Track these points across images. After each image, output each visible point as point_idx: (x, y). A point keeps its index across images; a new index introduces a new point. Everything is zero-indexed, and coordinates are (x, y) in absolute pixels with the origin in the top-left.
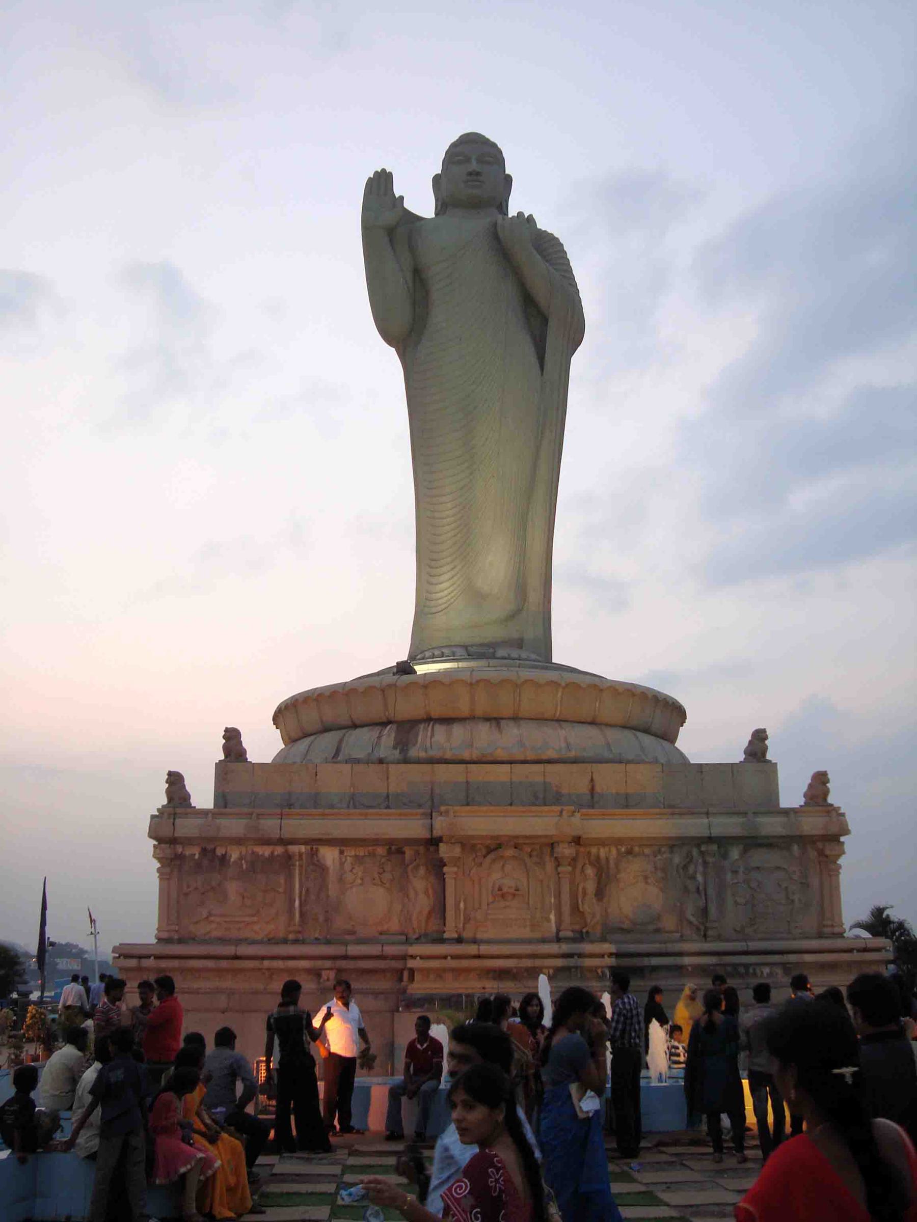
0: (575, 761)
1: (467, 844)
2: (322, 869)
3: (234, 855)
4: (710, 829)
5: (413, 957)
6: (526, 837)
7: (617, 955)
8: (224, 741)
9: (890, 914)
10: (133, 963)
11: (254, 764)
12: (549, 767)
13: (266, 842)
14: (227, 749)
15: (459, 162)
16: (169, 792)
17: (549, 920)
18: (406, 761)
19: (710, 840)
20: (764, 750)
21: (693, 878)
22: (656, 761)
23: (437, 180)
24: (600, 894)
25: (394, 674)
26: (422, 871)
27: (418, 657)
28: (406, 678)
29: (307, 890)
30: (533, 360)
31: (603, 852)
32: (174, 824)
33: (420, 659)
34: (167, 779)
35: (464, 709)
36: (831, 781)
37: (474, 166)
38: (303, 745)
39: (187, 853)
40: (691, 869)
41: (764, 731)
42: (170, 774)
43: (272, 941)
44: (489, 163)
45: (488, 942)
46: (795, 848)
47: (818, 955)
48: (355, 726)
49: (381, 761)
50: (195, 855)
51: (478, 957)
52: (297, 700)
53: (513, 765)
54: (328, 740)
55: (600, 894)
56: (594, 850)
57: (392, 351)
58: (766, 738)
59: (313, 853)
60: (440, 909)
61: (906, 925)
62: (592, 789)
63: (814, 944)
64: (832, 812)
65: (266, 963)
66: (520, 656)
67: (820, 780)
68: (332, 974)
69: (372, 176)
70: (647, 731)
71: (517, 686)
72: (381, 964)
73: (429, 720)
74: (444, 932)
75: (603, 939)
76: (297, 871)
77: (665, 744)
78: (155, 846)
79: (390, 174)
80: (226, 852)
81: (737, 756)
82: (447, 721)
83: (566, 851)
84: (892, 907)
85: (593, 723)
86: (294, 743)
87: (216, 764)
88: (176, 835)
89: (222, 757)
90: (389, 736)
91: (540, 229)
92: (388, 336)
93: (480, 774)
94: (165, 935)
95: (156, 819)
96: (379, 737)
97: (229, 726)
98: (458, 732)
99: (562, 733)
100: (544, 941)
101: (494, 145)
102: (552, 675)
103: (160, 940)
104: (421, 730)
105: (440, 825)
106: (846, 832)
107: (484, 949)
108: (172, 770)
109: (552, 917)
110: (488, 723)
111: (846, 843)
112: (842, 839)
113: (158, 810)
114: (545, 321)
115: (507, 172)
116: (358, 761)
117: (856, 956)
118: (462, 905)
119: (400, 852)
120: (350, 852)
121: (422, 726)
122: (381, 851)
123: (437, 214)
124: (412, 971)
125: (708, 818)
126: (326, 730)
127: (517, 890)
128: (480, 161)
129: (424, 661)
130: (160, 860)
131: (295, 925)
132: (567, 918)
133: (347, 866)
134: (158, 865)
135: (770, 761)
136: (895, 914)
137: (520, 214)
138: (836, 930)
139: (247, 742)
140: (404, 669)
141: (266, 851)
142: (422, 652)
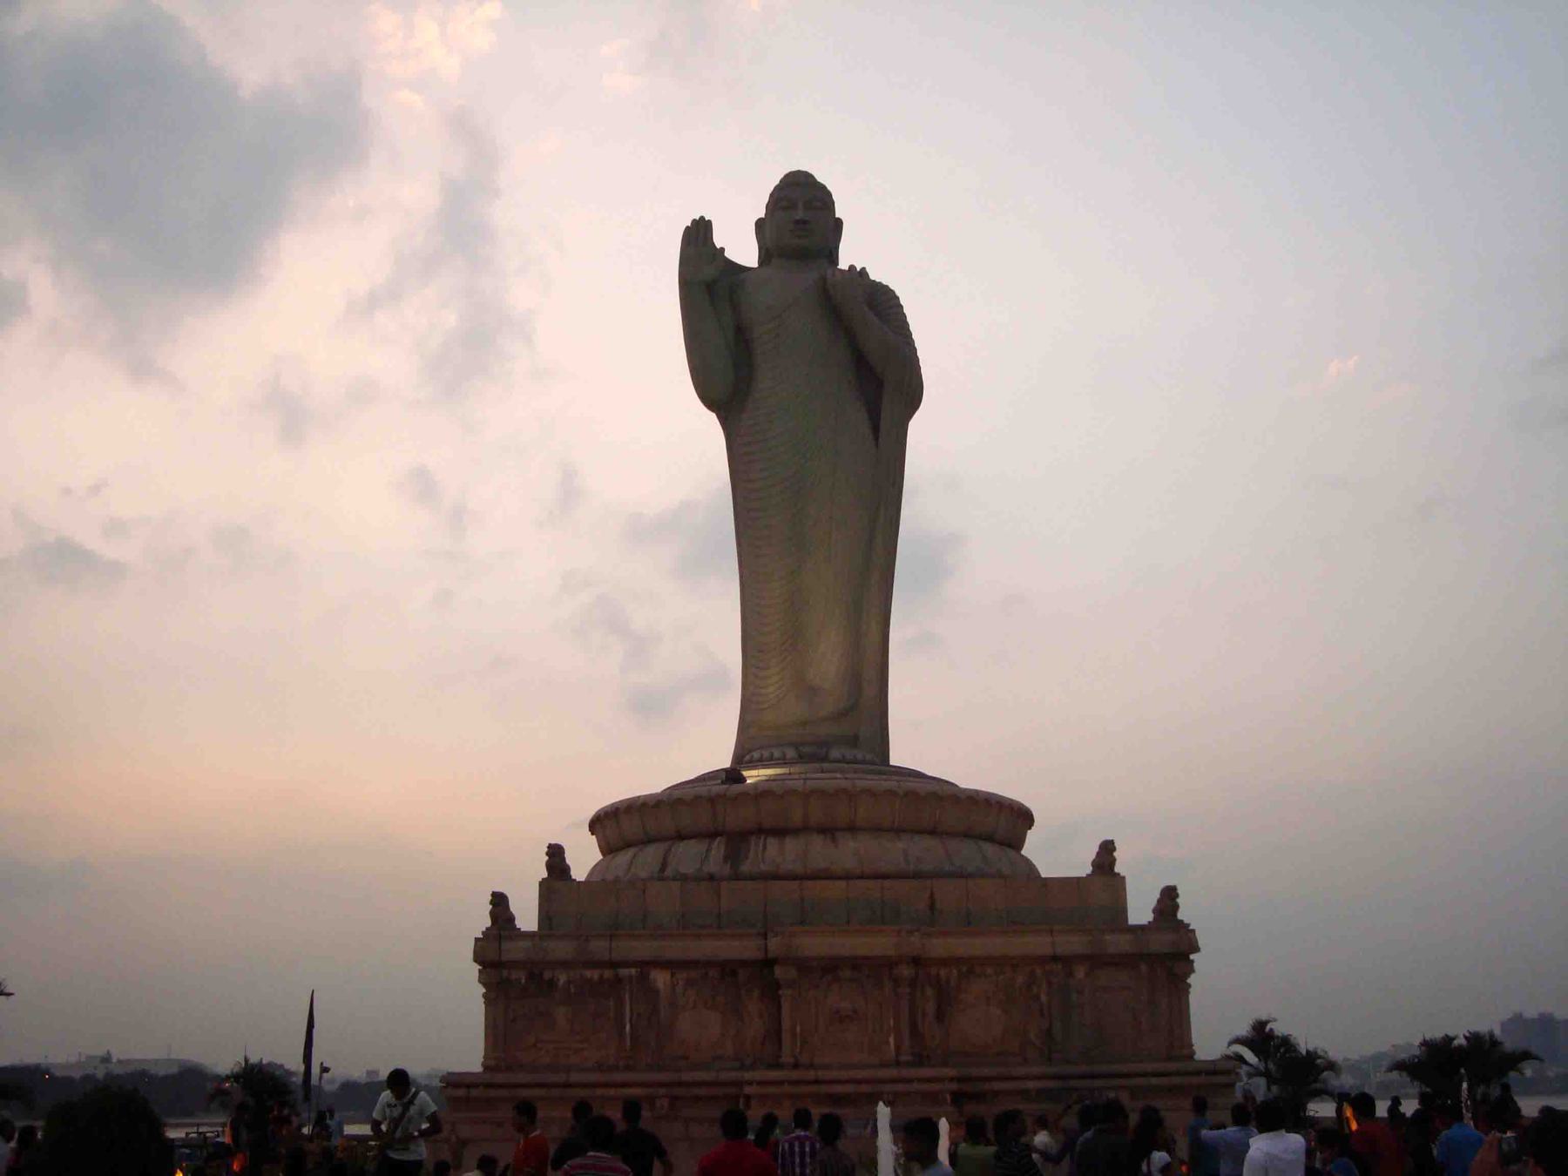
0: (917, 875)
1: (804, 966)
3: (562, 979)
5: (750, 1083)
6: (866, 958)
7: (960, 1080)
9: (1273, 1027)
10: (461, 1092)
11: (579, 882)
12: (887, 883)
14: (549, 866)
15: (785, 209)
16: (492, 914)
17: (888, 1043)
18: (737, 877)
19: (1055, 958)
21: (1037, 997)
22: (1000, 875)
23: (760, 224)
24: (940, 1016)
25: (723, 783)
26: (756, 993)
27: (747, 758)
28: (737, 788)
29: (639, 1015)
30: (866, 429)
31: (943, 972)
32: (500, 948)
33: (746, 763)
34: (492, 901)
35: (797, 817)
38: (623, 858)
40: (1035, 990)
41: (1112, 842)
43: (600, 1067)
45: (827, 1067)
46: (1144, 968)
48: (681, 837)
49: (711, 878)
51: (816, 1082)
52: (617, 809)
53: (851, 882)
54: (652, 853)
55: (940, 1016)
56: (933, 971)
57: (713, 416)
58: (1114, 849)
59: (643, 978)
60: (774, 1034)
61: (1292, 1039)
62: (932, 907)
64: (1184, 931)
66: (855, 756)
67: (1169, 896)
68: (666, 1103)
70: (990, 838)
71: (850, 796)
73: (762, 831)
74: (780, 1057)
75: (945, 1064)
76: (627, 996)
77: (1011, 853)
78: (480, 971)
79: (710, 222)
80: (553, 977)
82: (780, 832)
83: (906, 971)
84: (1275, 1020)
85: (933, 832)
86: (611, 856)
88: (504, 958)
89: (545, 874)
90: (718, 848)
92: (709, 398)
93: (816, 889)
94: (492, 1063)
96: (708, 850)
97: (553, 842)
98: (792, 845)
99: (900, 845)
100: (884, 1065)
102: (890, 784)
103: (486, 1067)
104: (753, 843)
105: (774, 944)
106: (1196, 949)
107: (821, 1074)
109: (891, 1040)
110: (822, 837)
112: (1192, 957)
113: (483, 933)
114: (880, 385)
115: (837, 216)
116: (684, 878)
117: (1202, 1079)
118: (798, 1029)
119: (734, 973)
120: (682, 976)
121: (753, 839)
122: (713, 973)
124: (748, 1098)
126: (649, 840)
127: (855, 1012)
129: (753, 764)
130: (485, 985)
131: (626, 1050)
132: (907, 1043)
133: (679, 990)
134: (484, 990)
135: (1119, 874)
136: (1279, 1028)
137: (852, 267)
138: (1185, 1052)
139: (570, 858)
140: (732, 776)
141: (594, 974)
142: (750, 751)
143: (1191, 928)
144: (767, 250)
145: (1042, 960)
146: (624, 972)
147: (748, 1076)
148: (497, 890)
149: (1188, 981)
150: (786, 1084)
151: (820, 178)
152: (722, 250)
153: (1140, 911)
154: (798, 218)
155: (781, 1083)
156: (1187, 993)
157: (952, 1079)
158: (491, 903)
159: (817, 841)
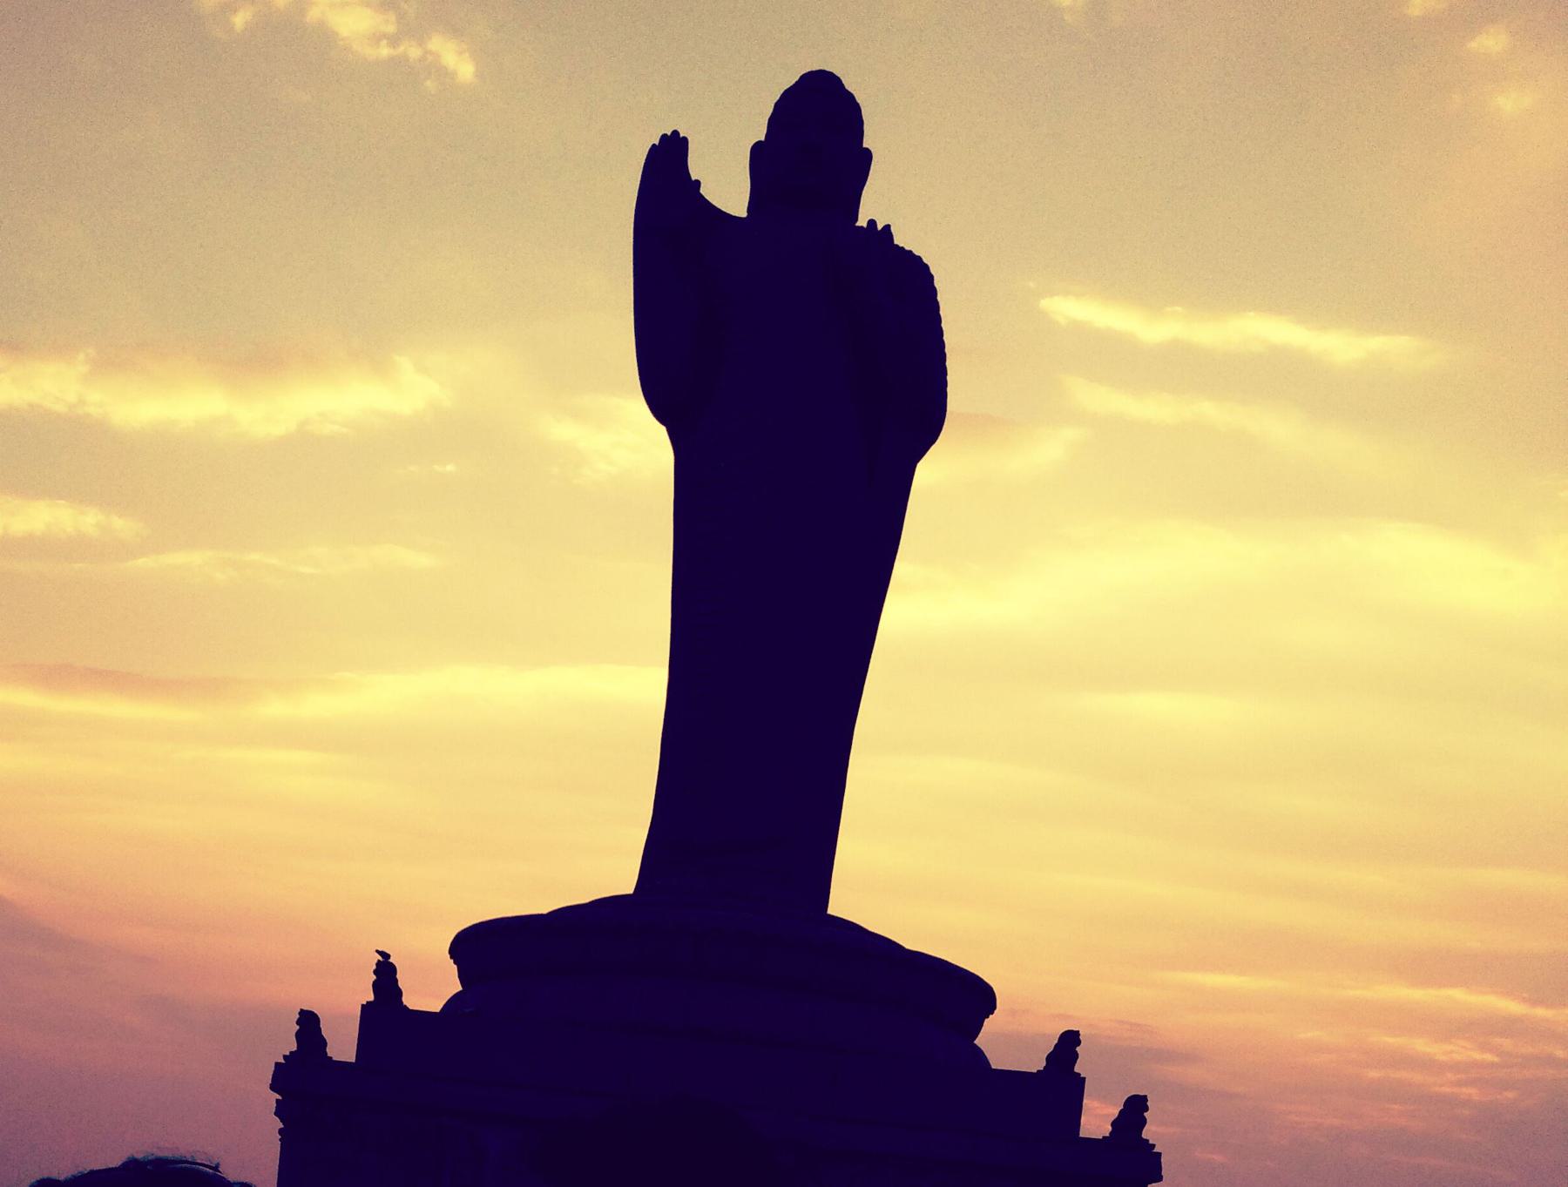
8: (375, 977)
42: (302, 1012)
58: (1079, 1043)
67: (1135, 1109)
79: (685, 140)
87: (363, 1005)
108: (305, 1009)
115: (865, 145)
151: (849, 85)
152: (698, 183)
153: (1097, 1119)
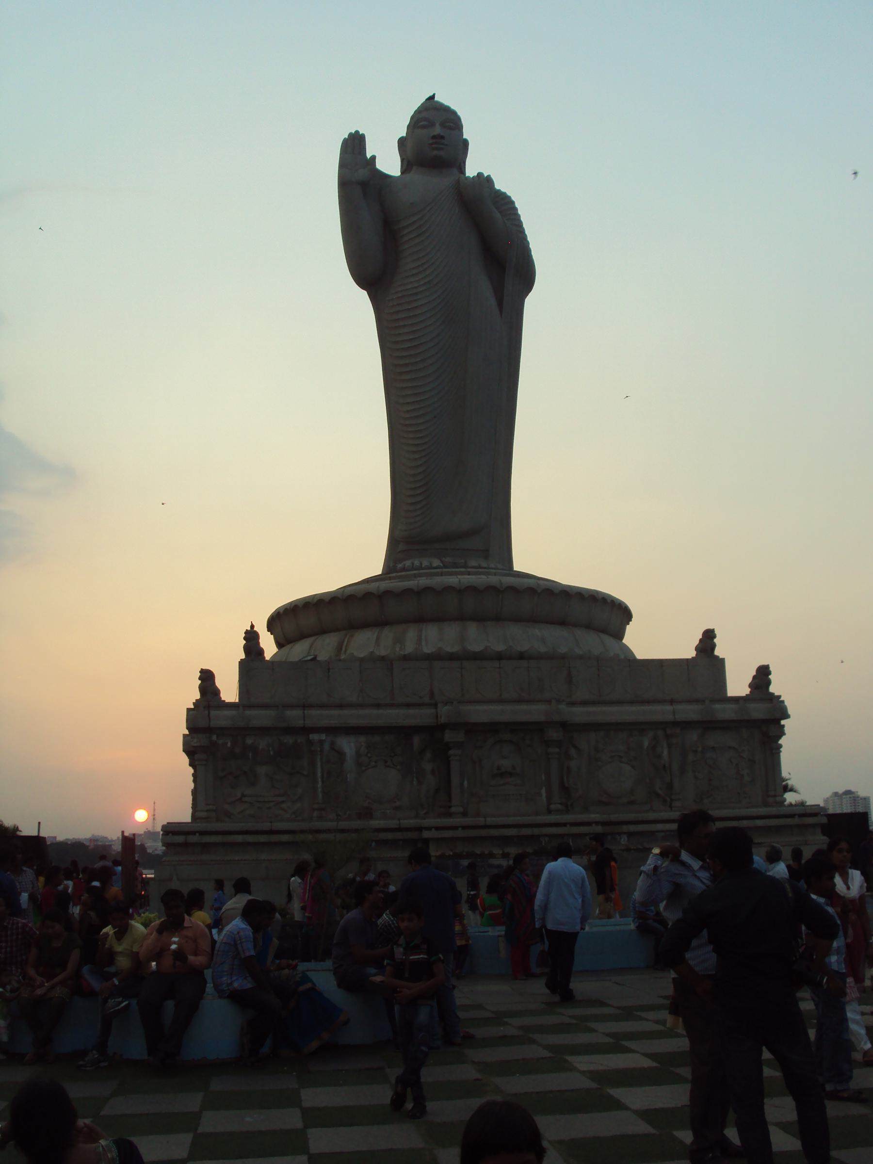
1: (473, 730)
2: (341, 755)
4: (674, 715)
5: (429, 829)
7: (604, 824)
8: (245, 642)
13: (290, 730)
14: (247, 649)
15: (424, 127)
19: (675, 724)
20: (713, 646)
23: (402, 142)
26: (428, 755)
34: (200, 676)
36: (772, 673)
37: (437, 130)
39: (220, 742)
44: (450, 128)
47: (767, 820)
50: (227, 743)
57: (365, 293)
63: (763, 811)
65: (322, 836)
69: (347, 137)
72: (398, 835)
74: (450, 807)
81: (688, 652)
83: (554, 734)
89: (243, 656)
91: (499, 190)
95: (191, 712)
101: (454, 113)
106: (786, 716)
108: (204, 668)
109: (543, 791)
111: (786, 726)
112: (783, 722)
115: (464, 137)
117: (796, 821)
123: (403, 172)
124: (426, 841)
125: (672, 705)
128: (442, 125)
137: (480, 175)
138: (778, 799)
141: (289, 740)
143: (782, 699)
144: (409, 162)
145: (663, 725)
146: (314, 737)
147: (427, 822)
148: (206, 667)
149: (780, 742)
150: (460, 829)
151: (452, 107)
154: (435, 133)
155: (455, 828)
156: (779, 753)
157: (597, 823)
158: (200, 679)
159: (472, 629)
